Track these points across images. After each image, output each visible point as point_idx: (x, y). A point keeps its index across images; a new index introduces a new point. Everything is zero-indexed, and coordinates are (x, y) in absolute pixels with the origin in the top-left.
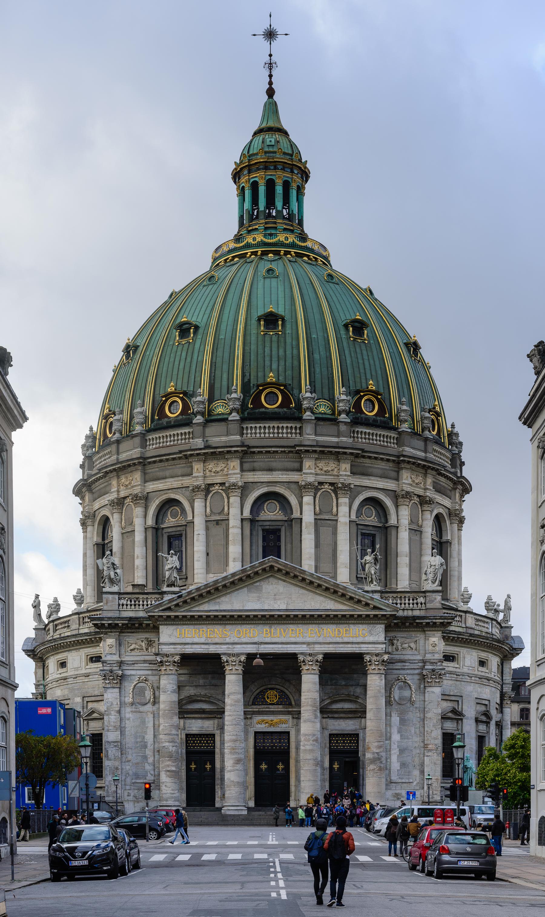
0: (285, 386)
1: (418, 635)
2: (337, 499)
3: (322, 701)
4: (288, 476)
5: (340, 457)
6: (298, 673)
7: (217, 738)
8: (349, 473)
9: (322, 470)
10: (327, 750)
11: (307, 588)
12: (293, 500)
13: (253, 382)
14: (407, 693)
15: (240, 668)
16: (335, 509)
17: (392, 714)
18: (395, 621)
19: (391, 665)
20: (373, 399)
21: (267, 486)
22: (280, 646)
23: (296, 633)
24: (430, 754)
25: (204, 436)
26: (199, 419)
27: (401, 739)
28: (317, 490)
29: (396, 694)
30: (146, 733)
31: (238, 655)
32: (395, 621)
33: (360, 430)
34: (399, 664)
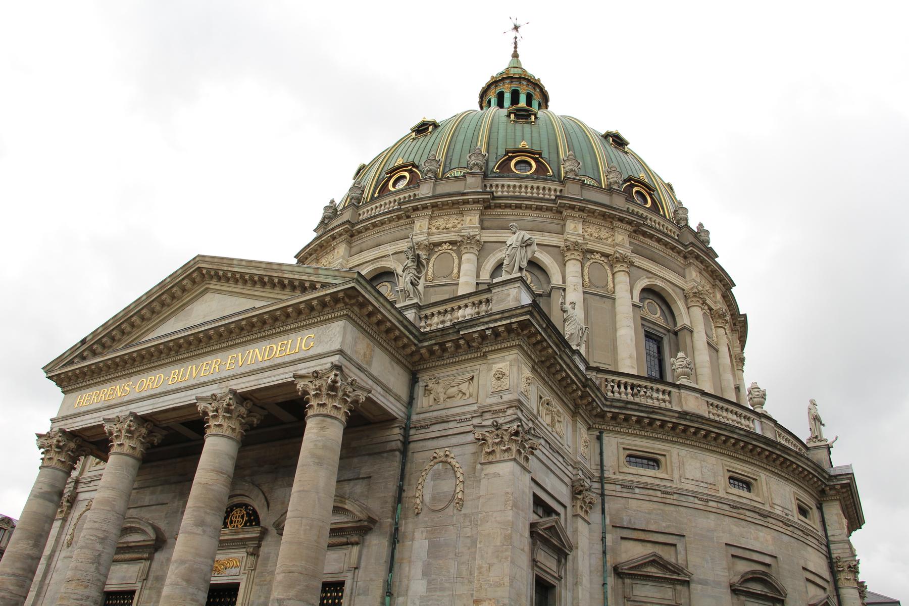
0: (414, 165)
1: (477, 367)
2: (460, 259)
4: (397, 246)
5: (462, 207)
9: (439, 229)
11: (244, 292)
17: (418, 535)
18: (426, 344)
19: (423, 431)
21: (372, 264)
23: (210, 368)
27: (429, 590)
32: (426, 344)
33: (500, 183)
34: (437, 427)
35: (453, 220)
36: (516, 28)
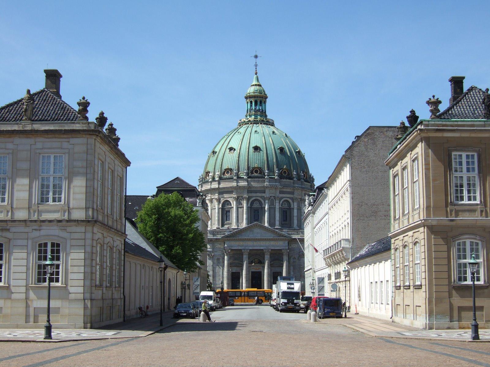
0: (260, 168)
3: (270, 262)
6: (264, 254)
7: (241, 273)
8: (279, 193)
10: (272, 277)
12: (263, 202)
13: (251, 166)
14: (295, 260)
15: (247, 254)
16: (275, 205)
20: (286, 171)
22: (259, 247)
24: (302, 278)
25: (237, 183)
26: (235, 178)
28: (270, 198)
29: (292, 260)
30: (220, 272)
31: (247, 250)
35: (274, 190)
36: (256, 57)
